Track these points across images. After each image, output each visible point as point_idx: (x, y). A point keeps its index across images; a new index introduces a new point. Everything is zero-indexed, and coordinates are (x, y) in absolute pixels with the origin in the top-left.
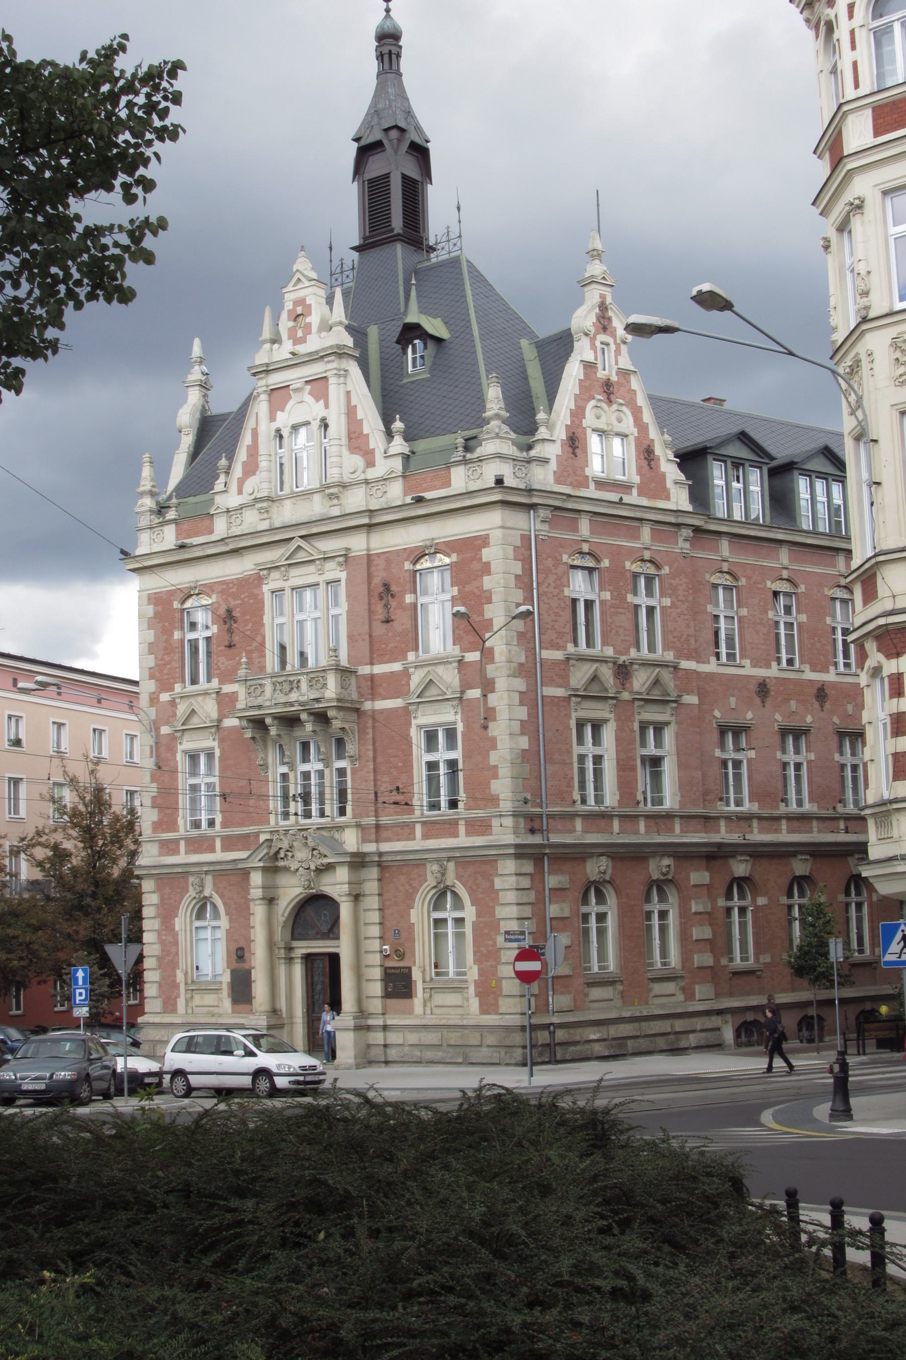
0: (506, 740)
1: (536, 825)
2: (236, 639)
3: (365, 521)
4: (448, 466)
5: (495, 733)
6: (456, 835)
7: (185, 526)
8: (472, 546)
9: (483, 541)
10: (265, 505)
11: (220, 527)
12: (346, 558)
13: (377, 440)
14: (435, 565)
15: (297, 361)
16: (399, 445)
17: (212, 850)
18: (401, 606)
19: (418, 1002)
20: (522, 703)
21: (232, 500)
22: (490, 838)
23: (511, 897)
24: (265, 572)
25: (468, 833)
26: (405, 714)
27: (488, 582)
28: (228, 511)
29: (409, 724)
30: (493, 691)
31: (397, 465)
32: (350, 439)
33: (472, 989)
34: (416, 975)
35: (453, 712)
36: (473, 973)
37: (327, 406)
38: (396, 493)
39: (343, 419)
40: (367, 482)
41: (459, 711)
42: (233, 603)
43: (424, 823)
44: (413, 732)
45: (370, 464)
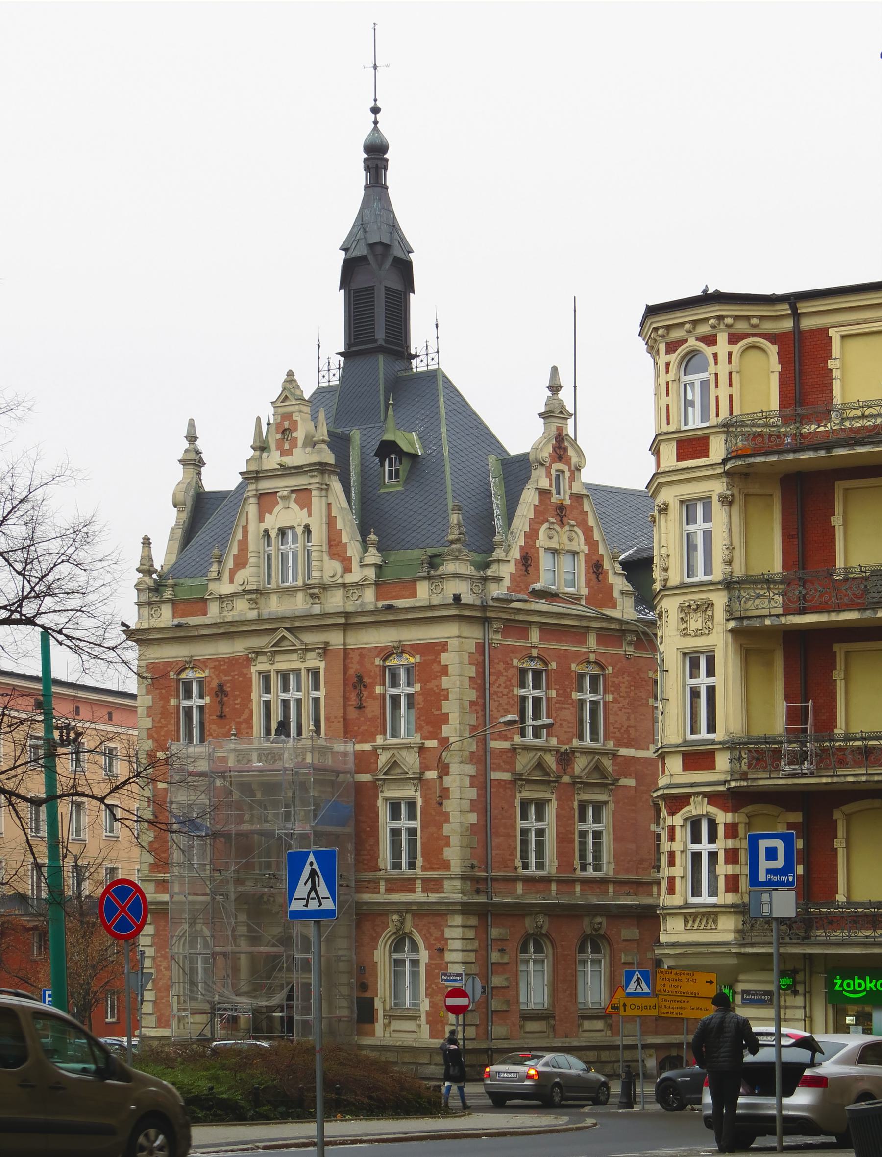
0: (459, 815)
1: (482, 887)
2: (227, 710)
3: (343, 621)
4: (415, 581)
5: (448, 810)
7: (182, 607)
8: (433, 651)
9: (443, 647)
10: (254, 596)
11: (213, 611)
12: (325, 650)
13: (353, 550)
14: (402, 663)
15: (285, 471)
16: (373, 556)
19: (379, 1026)
20: (472, 786)
21: (226, 588)
23: (457, 945)
24: (253, 655)
25: (424, 891)
26: (374, 788)
27: (445, 682)
28: (220, 597)
30: (447, 774)
31: (371, 573)
32: (330, 546)
34: (378, 1004)
35: (413, 789)
37: (310, 515)
38: (369, 596)
39: (324, 526)
40: (344, 585)
41: (419, 788)
43: (386, 880)
44: (380, 803)
45: (347, 569)
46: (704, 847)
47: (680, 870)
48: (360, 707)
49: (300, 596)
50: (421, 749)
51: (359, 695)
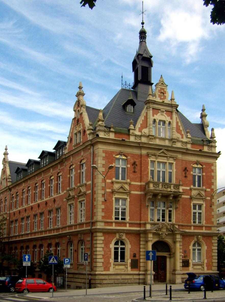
2: (136, 170)
3: (185, 151)
11: (132, 139)
14: (198, 167)
16: (189, 136)
17: (126, 226)
18: (190, 174)
21: (137, 133)
22: (211, 231)
24: (151, 155)
29: (191, 203)
30: (213, 198)
33: (205, 265)
34: (190, 261)
36: (206, 261)
37: (171, 118)
42: (136, 160)
44: (192, 204)
45: (182, 138)
48: (186, 177)
49: (167, 141)
50: (205, 191)
51: (185, 173)
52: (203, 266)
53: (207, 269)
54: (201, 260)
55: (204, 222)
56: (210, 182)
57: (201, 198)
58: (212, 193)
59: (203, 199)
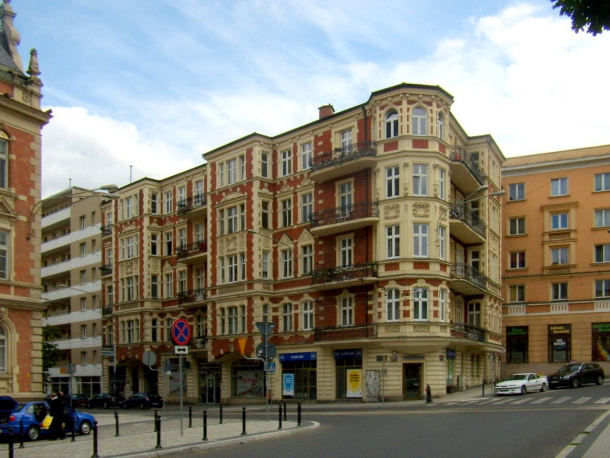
6: (9, 294)
22: (28, 298)
33: (15, 378)
36: (17, 370)
46: (394, 300)
47: (384, 308)
52: (10, 382)
53: (20, 387)
54: (4, 367)
55: (13, 274)
56: (27, 178)
57: (7, 214)
58: (32, 207)
59: (9, 217)
